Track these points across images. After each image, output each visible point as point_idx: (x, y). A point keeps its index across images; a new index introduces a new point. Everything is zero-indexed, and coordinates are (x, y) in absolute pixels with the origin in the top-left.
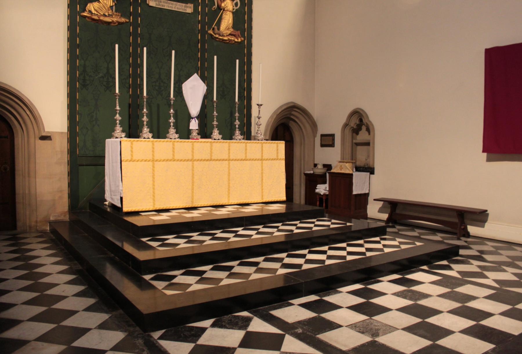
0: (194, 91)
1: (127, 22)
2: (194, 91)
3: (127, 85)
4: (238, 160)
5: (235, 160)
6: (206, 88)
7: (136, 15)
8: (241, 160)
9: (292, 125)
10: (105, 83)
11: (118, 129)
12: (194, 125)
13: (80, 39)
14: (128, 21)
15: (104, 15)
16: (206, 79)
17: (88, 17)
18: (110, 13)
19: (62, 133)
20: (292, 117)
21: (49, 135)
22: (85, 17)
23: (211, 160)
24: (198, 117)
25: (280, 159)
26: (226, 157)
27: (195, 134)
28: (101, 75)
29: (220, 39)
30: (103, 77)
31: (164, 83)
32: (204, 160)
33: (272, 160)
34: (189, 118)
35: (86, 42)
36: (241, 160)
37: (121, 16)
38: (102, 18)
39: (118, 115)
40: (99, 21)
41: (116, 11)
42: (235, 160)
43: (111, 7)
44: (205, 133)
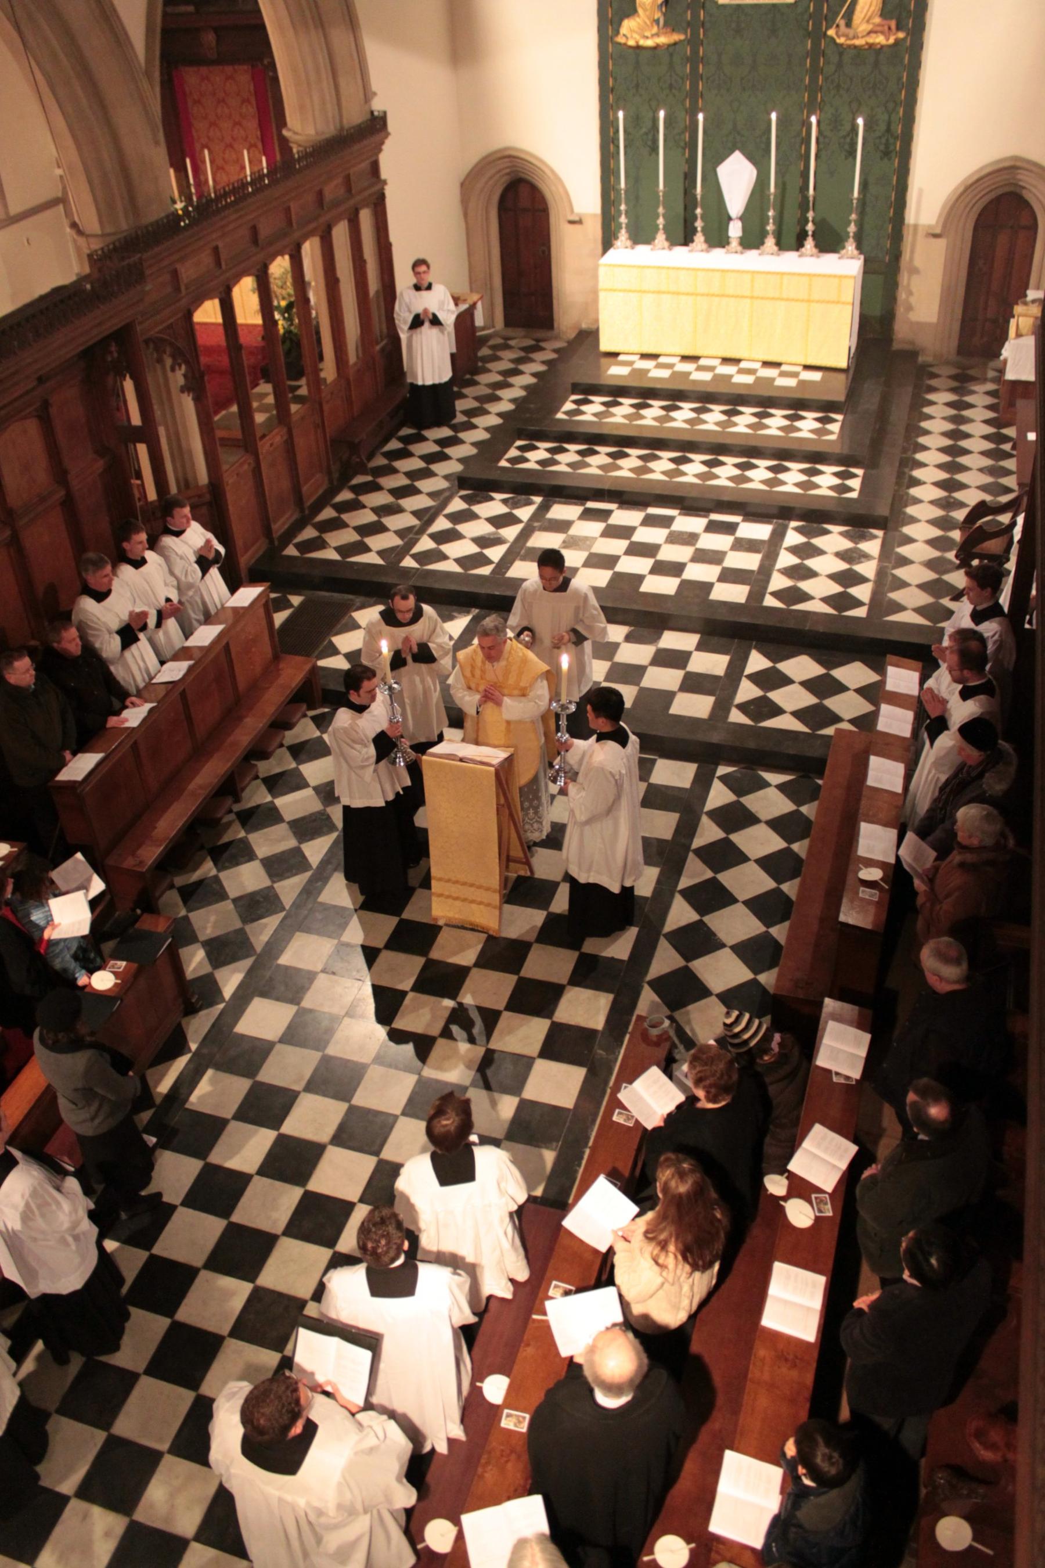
0: (736, 178)
1: (681, 41)
2: (736, 178)
3: (682, 144)
4: (767, 298)
5: (762, 298)
6: (755, 172)
7: (692, 25)
8: (773, 299)
9: (1026, 195)
10: (649, 143)
11: (623, 235)
12: (735, 230)
13: (615, 79)
14: (682, 37)
15: (647, 38)
16: (757, 157)
17: (625, 44)
18: (655, 30)
19: (595, 215)
20: (1021, 183)
21: (577, 219)
22: (620, 44)
23: (723, 296)
24: (741, 218)
25: (844, 303)
26: (748, 293)
27: (734, 244)
28: (644, 130)
29: (849, 46)
30: (646, 134)
31: (743, 136)
32: (713, 295)
33: (828, 302)
34: (730, 219)
35: (623, 77)
36: (773, 299)
37: (673, 30)
38: (642, 42)
39: (623, 216)
40: (638, 48)
41: (666, 25)
42: (762, 298)
43: (657, 22)
44: (752, 241)
